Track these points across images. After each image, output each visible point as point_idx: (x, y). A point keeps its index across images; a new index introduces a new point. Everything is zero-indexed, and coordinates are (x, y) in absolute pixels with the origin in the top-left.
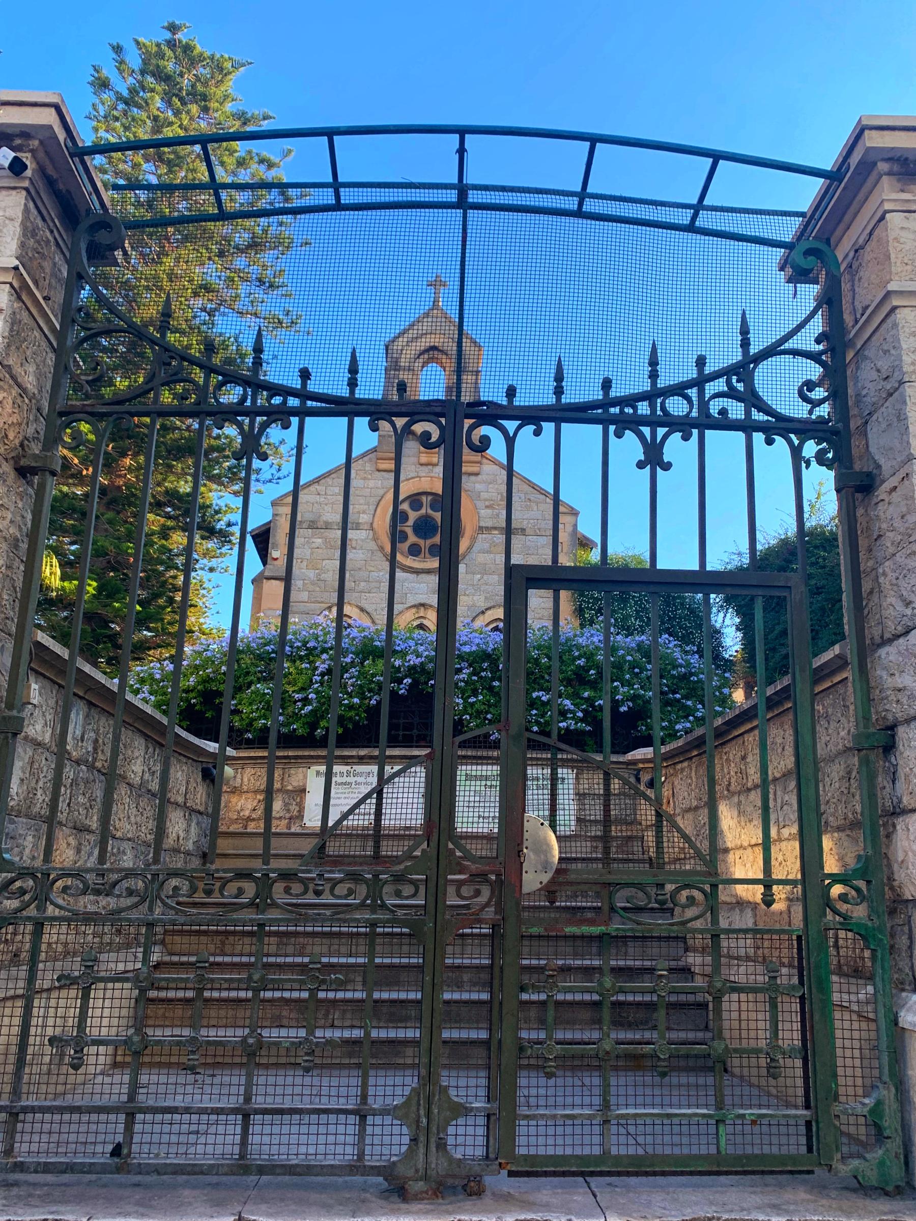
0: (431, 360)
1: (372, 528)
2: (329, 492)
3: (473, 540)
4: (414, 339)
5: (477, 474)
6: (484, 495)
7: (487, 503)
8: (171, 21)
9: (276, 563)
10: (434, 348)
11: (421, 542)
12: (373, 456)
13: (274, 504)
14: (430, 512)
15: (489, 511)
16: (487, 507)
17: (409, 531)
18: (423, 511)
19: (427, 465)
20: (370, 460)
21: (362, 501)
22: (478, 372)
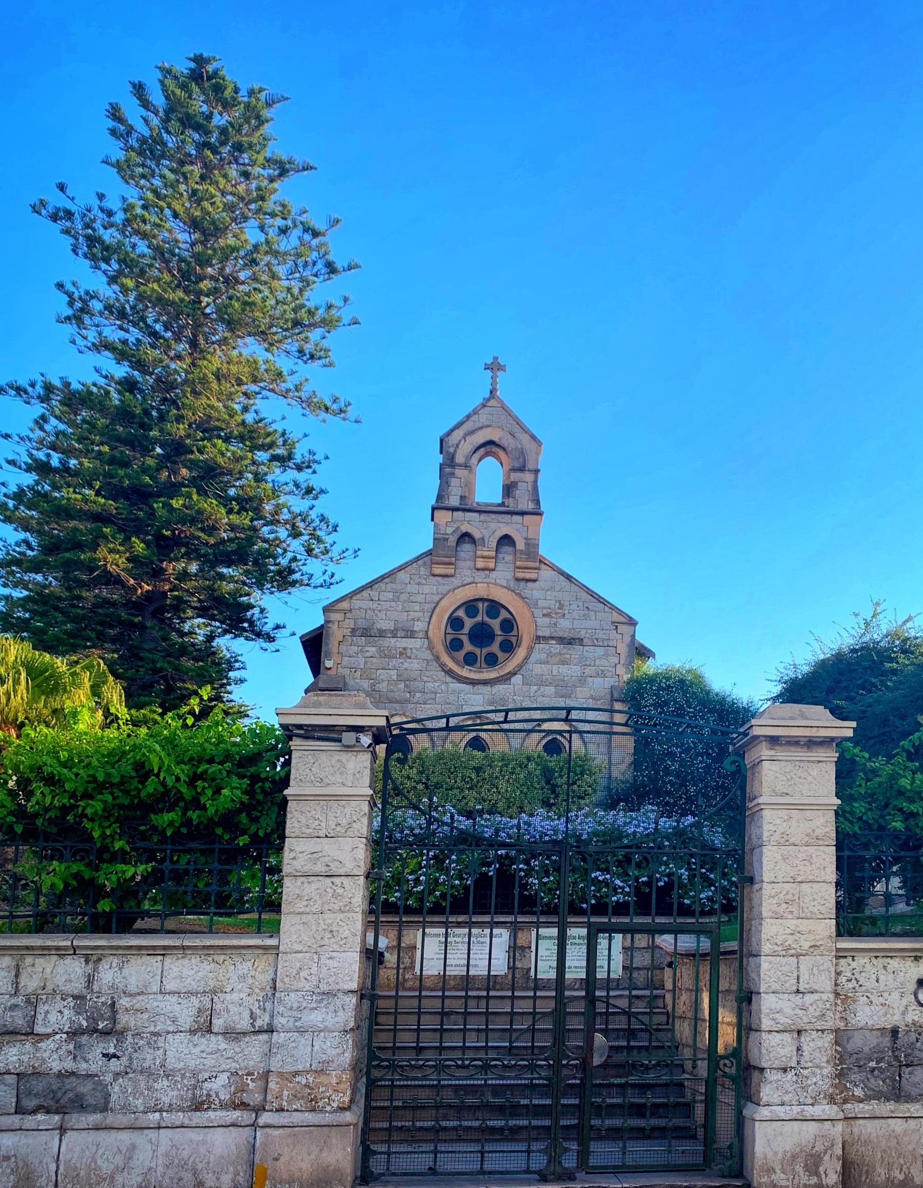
0: (487, 454)
1: (427, 637)
2: (382, 598)
3: (530, 650)
4: (472, 432)
5: (534, 581)
6: (542, 603)
7: (545, 611)
8: (198, 53)
9: (329, 672)
10: (491, 443)
11: (477, 651)
12: (427, 559)
13: (326, 610)
14: (486, 619)
15: (547, 620)
16: (544, 615)
17: (465, 639)
18: (479, 618)
20: (425, 564)
21: (417, 608)
22: (537, 472)
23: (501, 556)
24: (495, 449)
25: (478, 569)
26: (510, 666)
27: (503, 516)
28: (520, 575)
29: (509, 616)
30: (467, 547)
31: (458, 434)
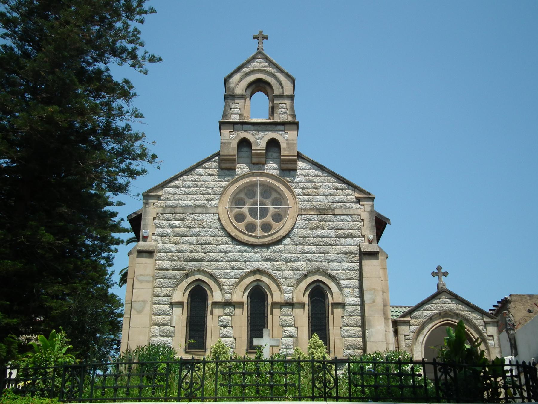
19: (257, 164)
23: (270, 154)
24: (262, 85)
25: (254, 164)
26: (282, 233)
27: (269, 126)
28: (285, 166)
29: (278, 196)
30: (245, 149)
31: (237, 76)
